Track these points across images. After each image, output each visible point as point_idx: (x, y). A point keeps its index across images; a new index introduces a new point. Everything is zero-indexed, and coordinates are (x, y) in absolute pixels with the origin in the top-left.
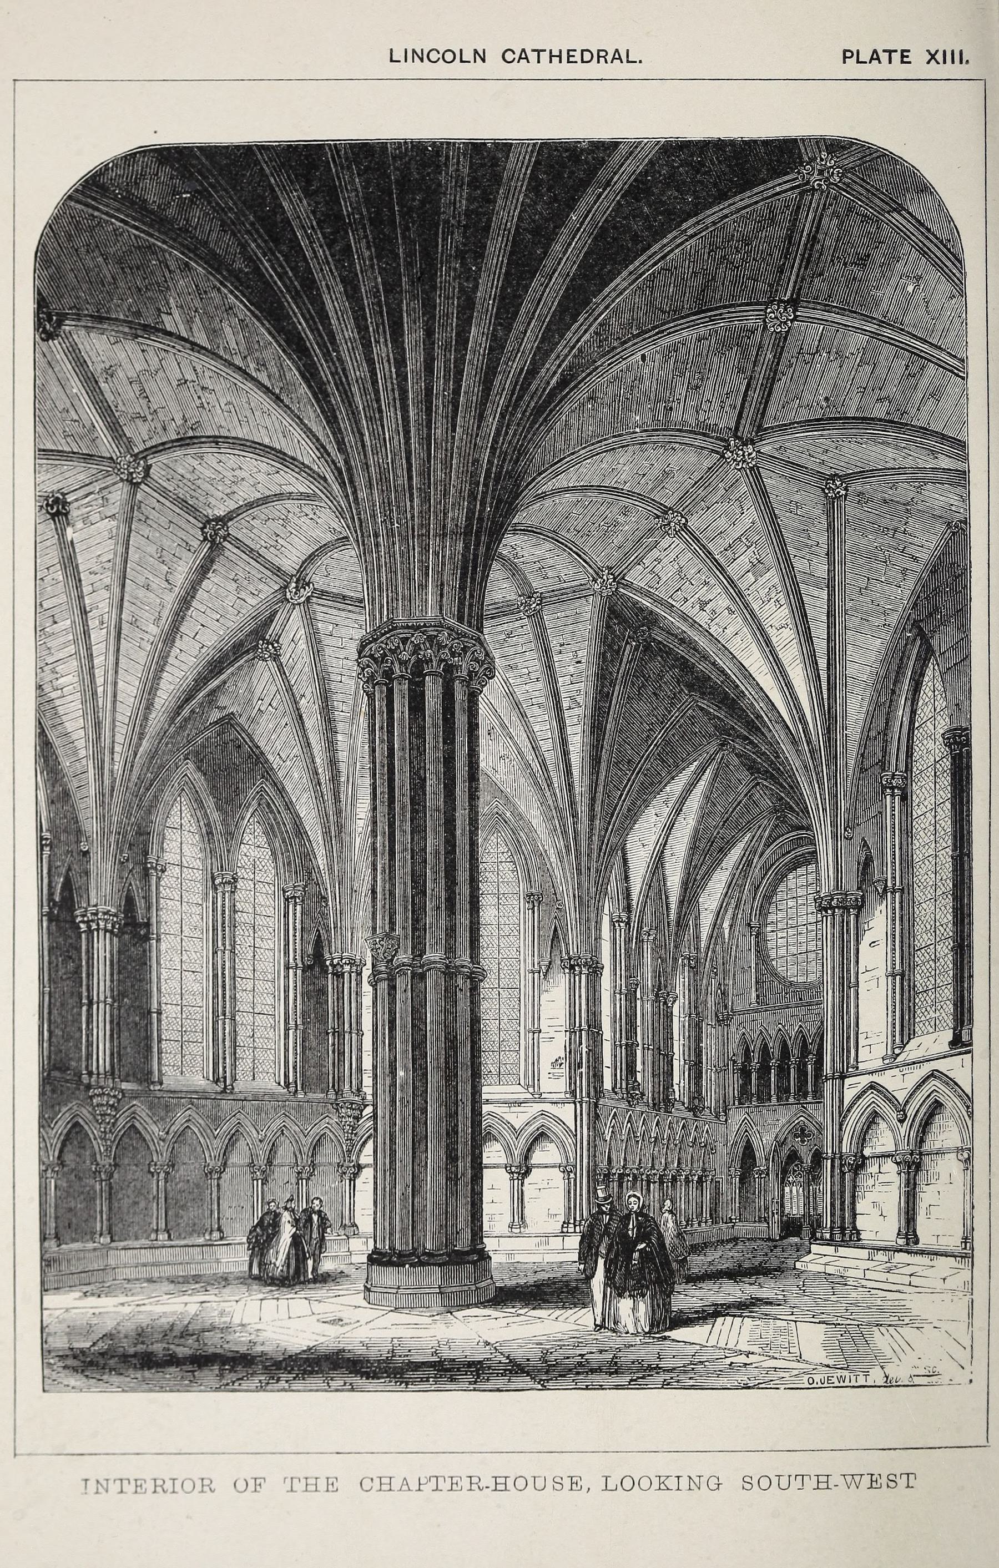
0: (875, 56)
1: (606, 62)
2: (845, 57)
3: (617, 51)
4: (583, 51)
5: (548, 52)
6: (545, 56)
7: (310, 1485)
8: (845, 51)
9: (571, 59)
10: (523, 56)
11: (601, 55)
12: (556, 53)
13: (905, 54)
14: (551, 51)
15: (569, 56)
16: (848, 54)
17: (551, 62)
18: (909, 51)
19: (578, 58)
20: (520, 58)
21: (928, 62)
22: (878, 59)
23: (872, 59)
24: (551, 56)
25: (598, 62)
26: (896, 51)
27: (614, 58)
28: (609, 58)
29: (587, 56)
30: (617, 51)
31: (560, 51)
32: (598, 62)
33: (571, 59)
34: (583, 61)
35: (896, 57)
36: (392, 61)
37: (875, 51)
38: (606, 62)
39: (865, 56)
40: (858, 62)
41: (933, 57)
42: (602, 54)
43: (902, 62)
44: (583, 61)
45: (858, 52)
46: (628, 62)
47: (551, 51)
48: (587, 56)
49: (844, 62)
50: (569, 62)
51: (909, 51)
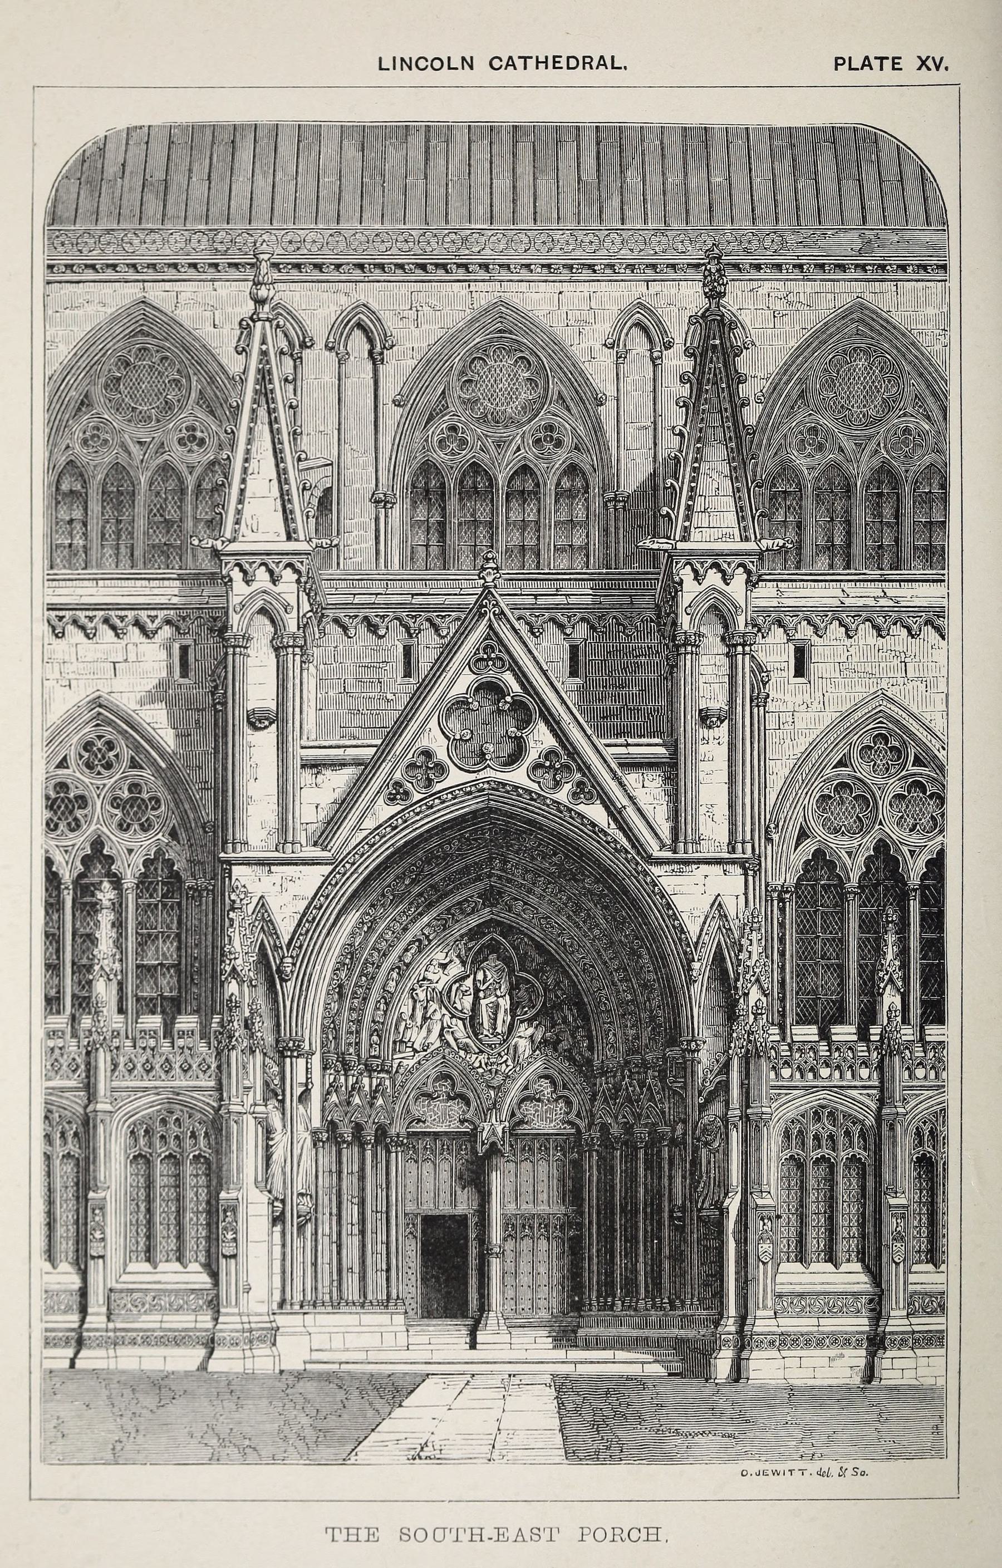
2: (837, 65)
3: (602, 57)
4: (568, 58)
5: (534, 59)
6: (531, 63)
7: (352, 1534)
8: (837, 59)
9: (557, 65)
10: (511, 63)
11: (586, 62)
12: (542, 59)
13: (896, 61)
14: (537, 58)
15: (555, 62)
16: (840, 61)
17: (537, 68)
18: (900, 58)
19: (563, 63)
20: (508, 65)
21: (919, 69)
22: (870, 65)
24: (538, 62)
25: (584, 68)
26: (887, 58)
29: (573, 63)
31: (546, 58)
32: (584, 68)
33: (557, 65)
34: (568, 68)
35: (888, 64)
37: (867, 58)
39: (857, 63)
40: (850, 69)
41: (924, 63)
42: (588, 60)
43: (894, 69)
44: (568, 68)
45: (850, 58)
47: (537, 58)
48: (573, 63)
49: (836, 69)
50: (554, 67)
51: (900, 58)
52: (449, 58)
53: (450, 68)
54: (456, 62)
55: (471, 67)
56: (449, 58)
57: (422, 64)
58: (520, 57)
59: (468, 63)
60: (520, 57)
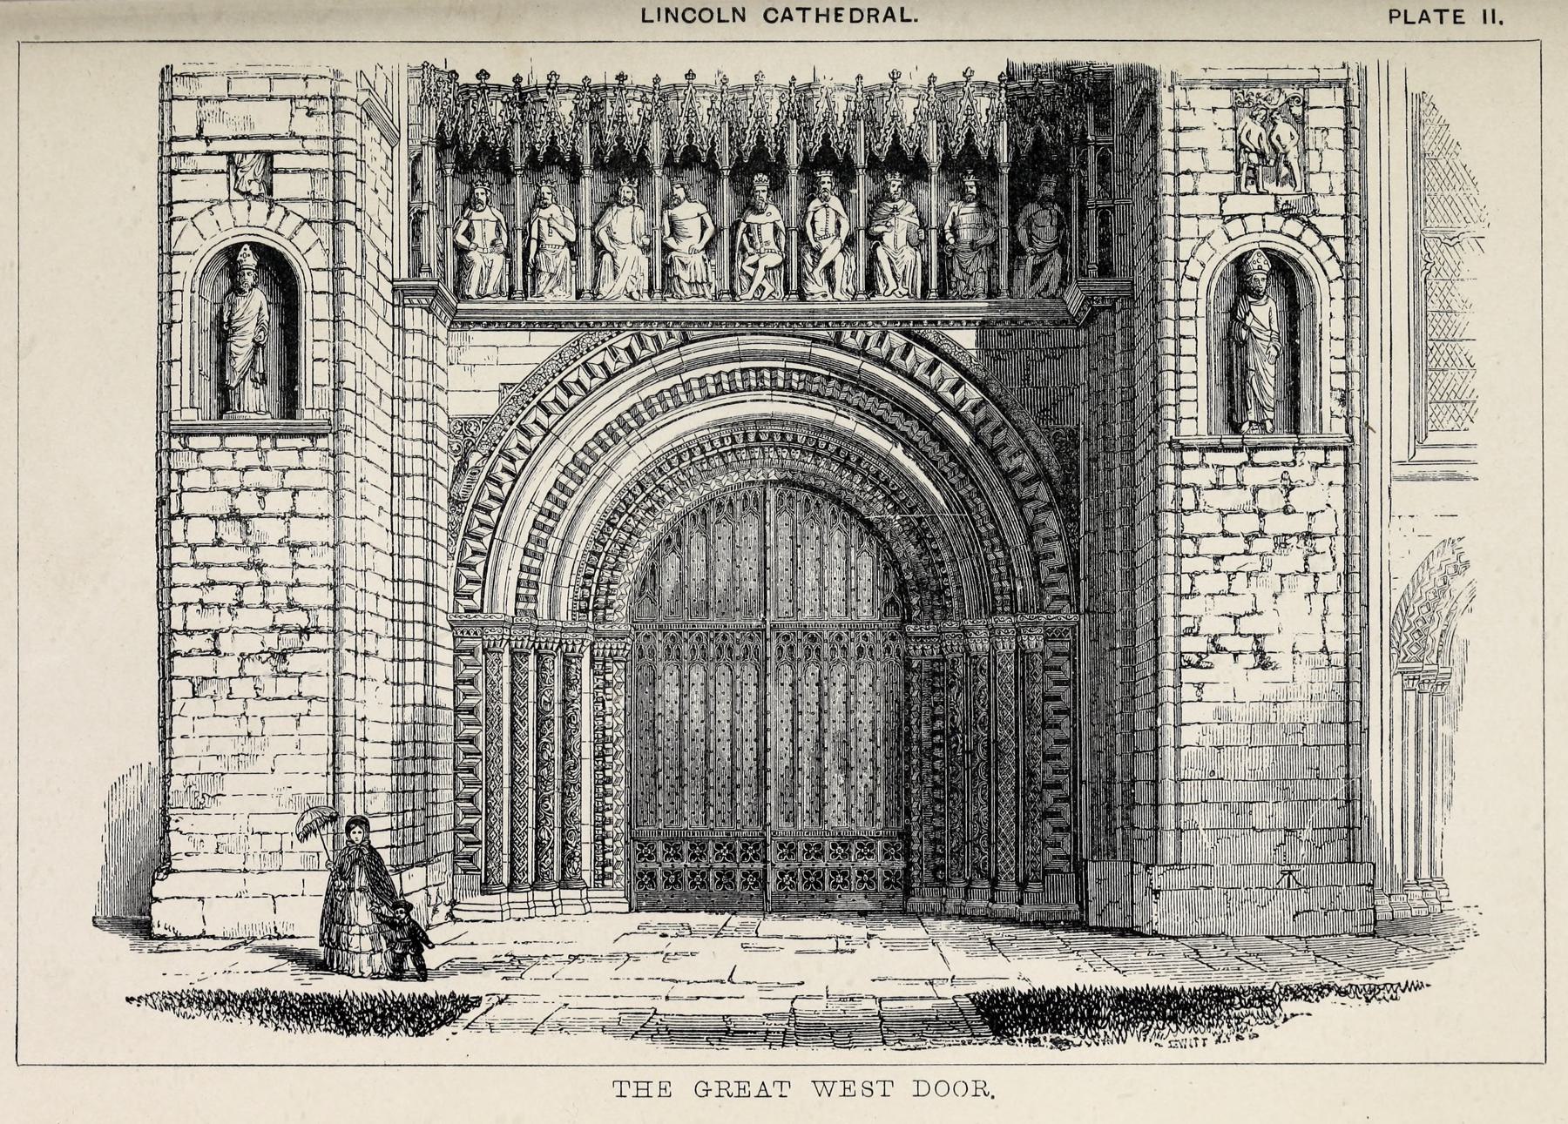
0: (1424, 17)
1: (877, 21)
3: (890, 9)
4: (852, 10)
6: (811, 15)
11: (873, 14)
14: (817, 10)
15: (837, 15)
17: (817, 21)
20: (784, 18)
23: (1421, 19)
24: (818, 15)
27: (886, 17)
28: (881, 17)
29: (857, 16)
30: (890, 9)
34: (852, 21)
36: (644, 21)
38: (877, 21)
42: (873, 13)
44: (852, 21)
46: (903, 20)
47: (817, 10)
48: (857, 16)
52: (719, 10)
53: (720, 21)
54: (727, 14)
55: (743, 19)
56: (719, 10)
57: (689, 15)
58: (798, 9)
59: (739, 14)
60: (798, 9)
